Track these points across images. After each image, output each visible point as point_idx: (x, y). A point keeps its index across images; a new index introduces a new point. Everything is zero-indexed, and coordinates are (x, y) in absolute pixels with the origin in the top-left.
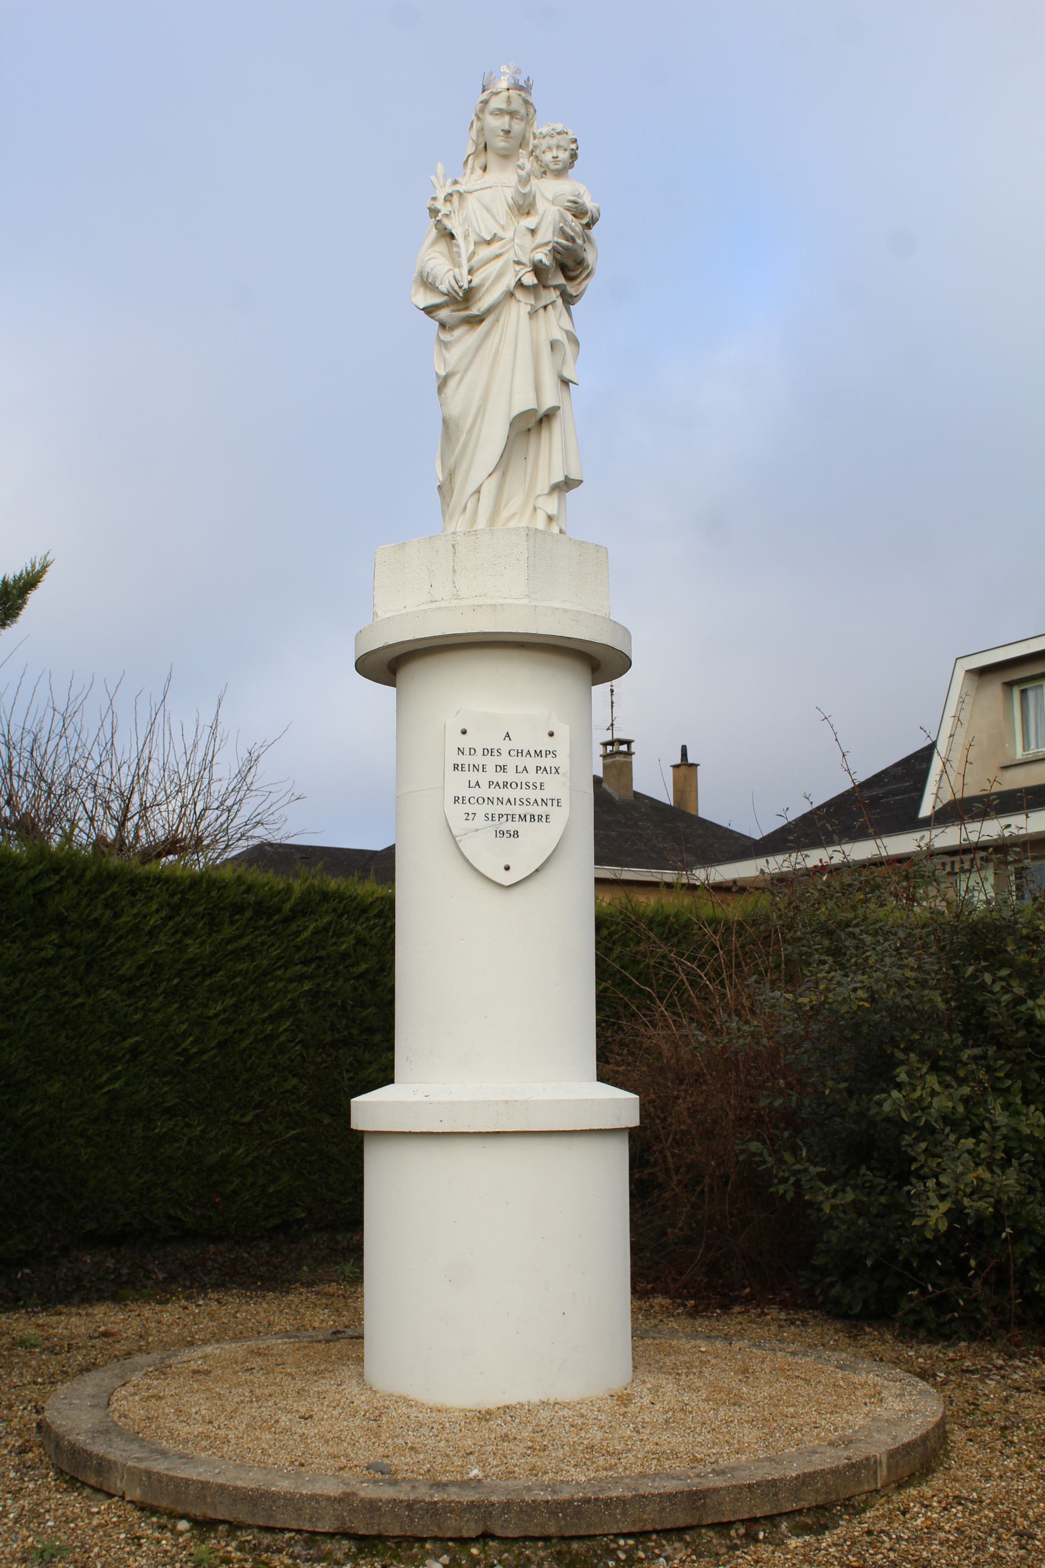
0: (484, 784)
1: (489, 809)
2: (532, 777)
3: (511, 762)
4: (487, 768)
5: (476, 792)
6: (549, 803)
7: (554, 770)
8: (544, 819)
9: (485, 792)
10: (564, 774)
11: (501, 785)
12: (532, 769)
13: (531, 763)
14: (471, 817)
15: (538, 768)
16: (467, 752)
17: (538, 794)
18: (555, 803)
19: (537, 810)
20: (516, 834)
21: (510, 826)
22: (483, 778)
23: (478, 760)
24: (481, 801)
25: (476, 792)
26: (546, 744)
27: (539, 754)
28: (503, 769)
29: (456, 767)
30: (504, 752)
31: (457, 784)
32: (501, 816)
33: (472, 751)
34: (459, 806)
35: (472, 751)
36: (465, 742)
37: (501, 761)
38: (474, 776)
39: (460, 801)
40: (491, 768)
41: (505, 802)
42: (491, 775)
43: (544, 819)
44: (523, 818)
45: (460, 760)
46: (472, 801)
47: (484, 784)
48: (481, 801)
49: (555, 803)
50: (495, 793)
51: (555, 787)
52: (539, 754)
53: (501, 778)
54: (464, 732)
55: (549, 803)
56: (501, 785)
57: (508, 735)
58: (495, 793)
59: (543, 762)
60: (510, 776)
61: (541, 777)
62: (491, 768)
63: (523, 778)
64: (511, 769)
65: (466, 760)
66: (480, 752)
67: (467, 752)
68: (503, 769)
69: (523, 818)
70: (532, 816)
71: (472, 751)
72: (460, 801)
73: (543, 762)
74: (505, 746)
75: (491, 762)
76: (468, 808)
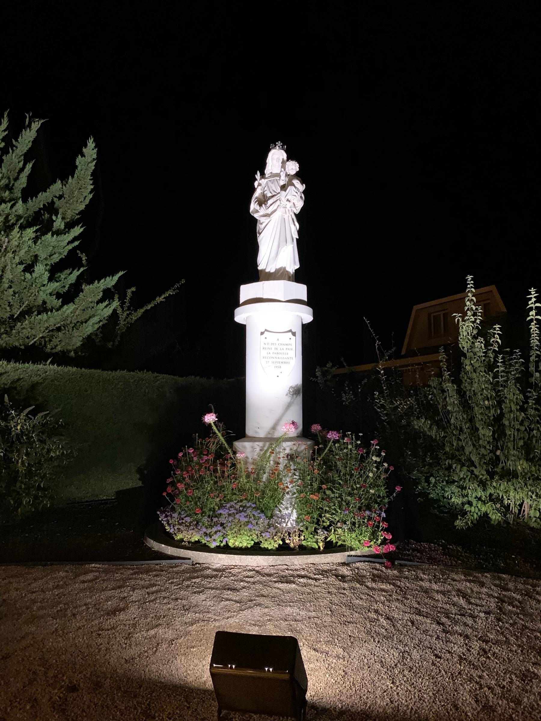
2: (285, 351)
3: (279, 347)
5: (269, 356)
9: (271, 355)
12: (285, 349)
13: (285, 347)
17: (286, 356)
22: (271, 351)
23: (270, 346)
25: (269, 356)
26: (289, 342)
27: (287, 345)
28: (277, 349)
29: (263, 348)
31: (264, 353)
35: (268, 344)
37: (276, 347)
38: (269, 351)
40: (273, 349)
44: (282, 363)
45: (265, 346)
50: (275, 356)
51: (292, 354)
52: (287, 345)
53: (276, 351)
58: (275, 356)
60: (279, 351)
62: (273, 349)
63: (282, 351)
64: (279, 349)
65: (267, 346)
68: (277, 349)
69: (282, 363)
74: (277, 342)
75: (273, 347)
76: (268, 360)
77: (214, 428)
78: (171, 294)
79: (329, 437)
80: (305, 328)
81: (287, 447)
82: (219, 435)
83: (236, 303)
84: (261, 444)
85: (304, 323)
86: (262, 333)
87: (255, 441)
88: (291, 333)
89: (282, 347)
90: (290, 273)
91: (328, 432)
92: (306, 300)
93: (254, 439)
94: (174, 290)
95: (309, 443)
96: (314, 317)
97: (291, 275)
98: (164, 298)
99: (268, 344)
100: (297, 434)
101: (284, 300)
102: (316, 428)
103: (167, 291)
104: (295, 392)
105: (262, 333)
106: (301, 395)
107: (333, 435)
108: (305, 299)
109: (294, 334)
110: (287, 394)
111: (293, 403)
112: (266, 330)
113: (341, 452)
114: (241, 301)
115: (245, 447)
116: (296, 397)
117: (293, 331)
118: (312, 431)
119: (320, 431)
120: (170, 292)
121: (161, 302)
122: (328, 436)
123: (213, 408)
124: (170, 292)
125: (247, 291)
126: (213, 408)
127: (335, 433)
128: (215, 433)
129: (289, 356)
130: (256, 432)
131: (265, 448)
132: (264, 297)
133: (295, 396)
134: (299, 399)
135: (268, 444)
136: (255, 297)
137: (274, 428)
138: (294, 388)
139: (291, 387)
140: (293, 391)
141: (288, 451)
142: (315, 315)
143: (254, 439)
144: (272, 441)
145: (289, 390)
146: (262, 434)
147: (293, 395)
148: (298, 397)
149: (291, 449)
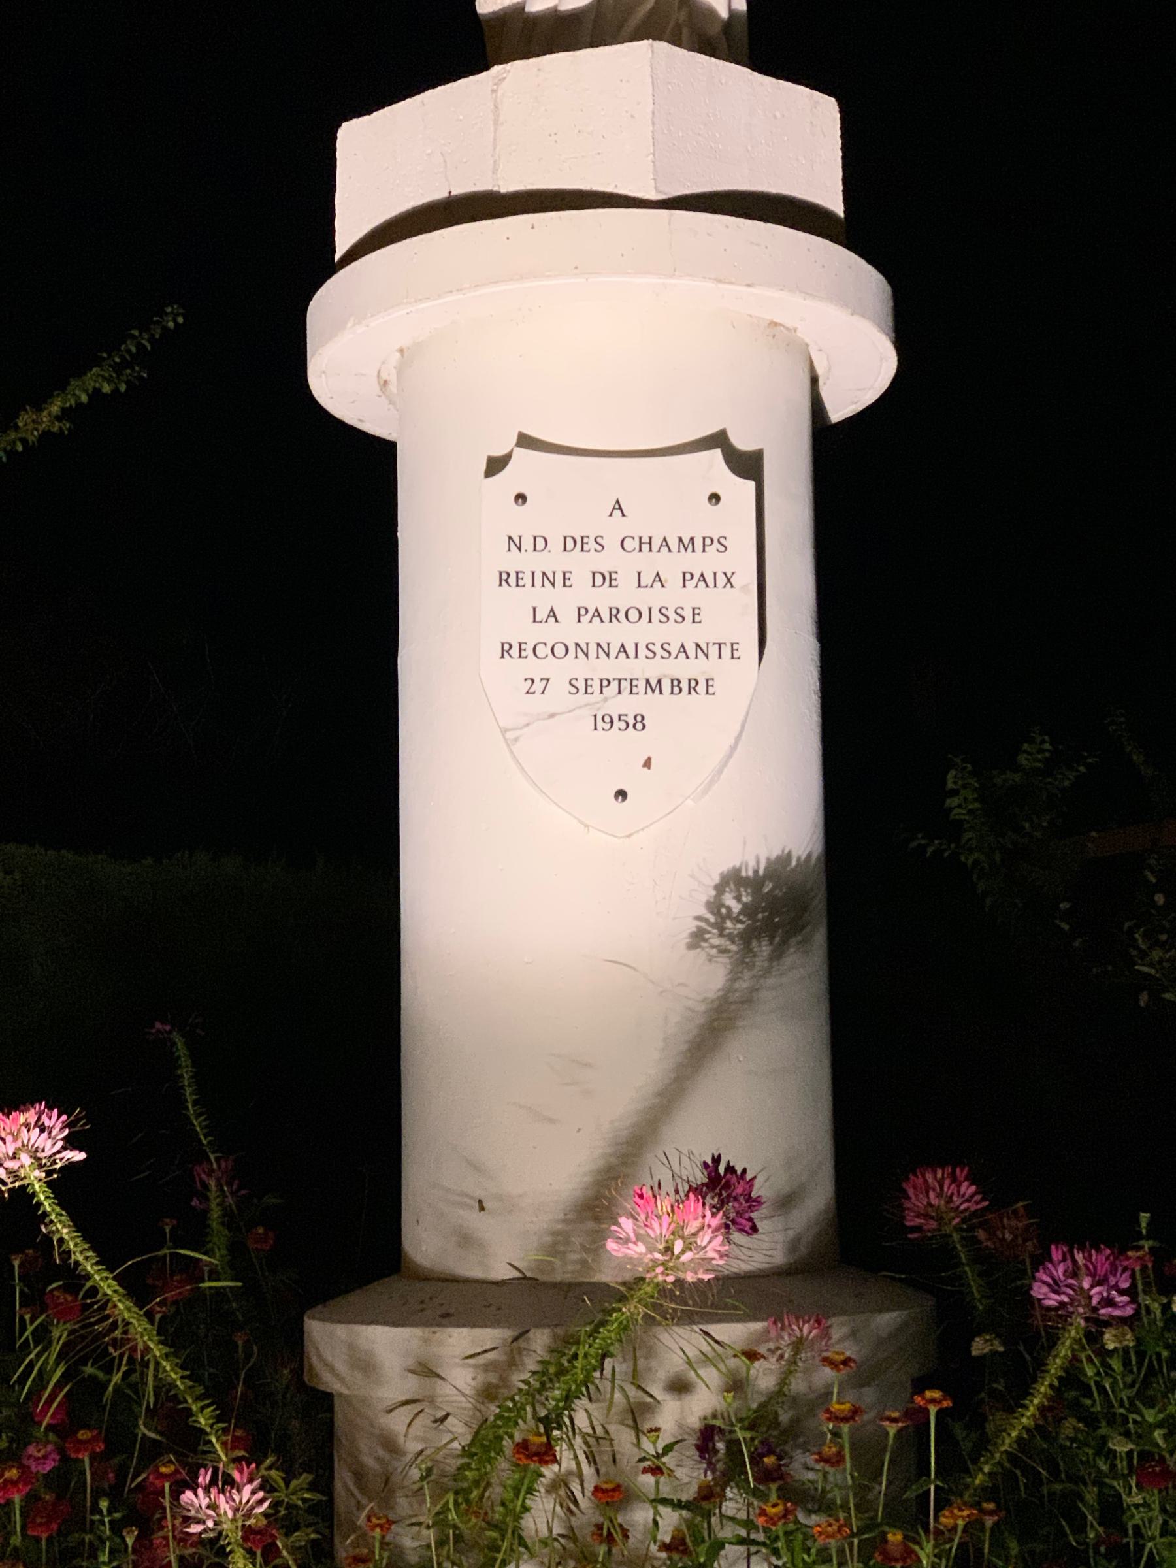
0: (567, 614)
1: (579, 668)
2: (673, 596)
3: (626, 565)
4: (573, 579)
5: (549, 633)
6: (713, 651)
7: (722, 580)
8: (702, 688)
9: (569, 631)
10: (745, 588)
11: (606, 617)
12: (673, 579)
13: (672, 564)
14: (538, 686)
15: (686, 577)
16: (527, 544)
17: (688, 634)
18: (726, 651)
19: (684, 669)
20: (640, 722)
21: (627, 705)
22: (565, 601)
23: (554, 561)
24: (560, 651)
25: (549, 633)
26: (707, 522)
28: (609, 579)
29: (504, 578)
30: (612, 543)
32: (605, 683)
33: (540, 543)
34: (512, 663)
35: (540, 543)
36: (523, 521)
37: (603, 562)
38: (545, 598)
39: (515, 651)
40: (581, 578)
41: (613, 654)
42: (584, 594)
43: (702, 688)
45: (513, 562)
46: (541, 650)
47: (567, 614)
48: (560, 651)
49: (726, 651)
50: (591, 632)
53: (603, 598)
54: (521, 498)
55: (713, 651)
56: (606, 617)
57: (618, 505)
58: (591, 632)
59: (696, 562)
60: (625, 595)
61: (695, 595)
62: (581, 578)
63: (654, 598)
64: (626, 580)
65: (526, 561)
66: (556, 544)
67: (527, 544)
68: (609, 579)
70: (676, 683)
71: (540, 543)
72: (515, 651)
73: (696, 562)
75: (581, 565)
77: (62, 1228)
78: (107, 388)
79: (1052, 1300)
80: (839, 451)
81: (691, 1380)
82: (107, 1286)
83: (318, 262)
84: (490, 1336)
85: (837, 413)
86: (495, 466)
87: (447, 1319)
88: (717, 453)
89: (650, 563)
90: (712, 13)
91: (1041, 1259)
92: (839, 209)
93: (451, 1299)
94: (118, 369)
95: (886, 1320)
96: (900, 343)
97: (714, 30)
98: (65, 414)
99: (540, 543)
100: (793, 1246)
101: (653, 196)
102: (942, 1197)
103: (80, 373)
104: (763, 913)
105: (495, 466)
106: (820, 938)
107: (1074, 1287)
108: (831, 197)
109: (747, 465)
110: (697, 938)
111: (748, 1000)
112: (526, 441)
113: (1150, 1416)
114: (343, 244)
115: (366, 1365)
116: (777, 955)
117: (743, 442)
118: (912, 1221)
119: (972, 1221)
120: (98, 381)
121: (46, 434)
122: (1039, 1291)
123: (181, 1049)
124: (98, 381)
125: (381, 158)
126: (181, 1049)
127: (1101, 1258)
128: (74, 1277)
129: (701, 634)
130: (466, 1240)
131: (518, 1378)
132: (507, 186)
133: (764, 949)
134: (802, 975)
135: (540, 1340)
136: (440, 194)
137: (596, 1208)
138: (755, 883)
139: (733, 880)
140: (747, 910)
141: (705, 1401)
142: (905, 334)
143: (451, 1299)
144: (570, 1314)
145: (715, 906)
146: (503, 1254)
147: (747, 938)
148: (792, 957)
149: (736, 1385)
